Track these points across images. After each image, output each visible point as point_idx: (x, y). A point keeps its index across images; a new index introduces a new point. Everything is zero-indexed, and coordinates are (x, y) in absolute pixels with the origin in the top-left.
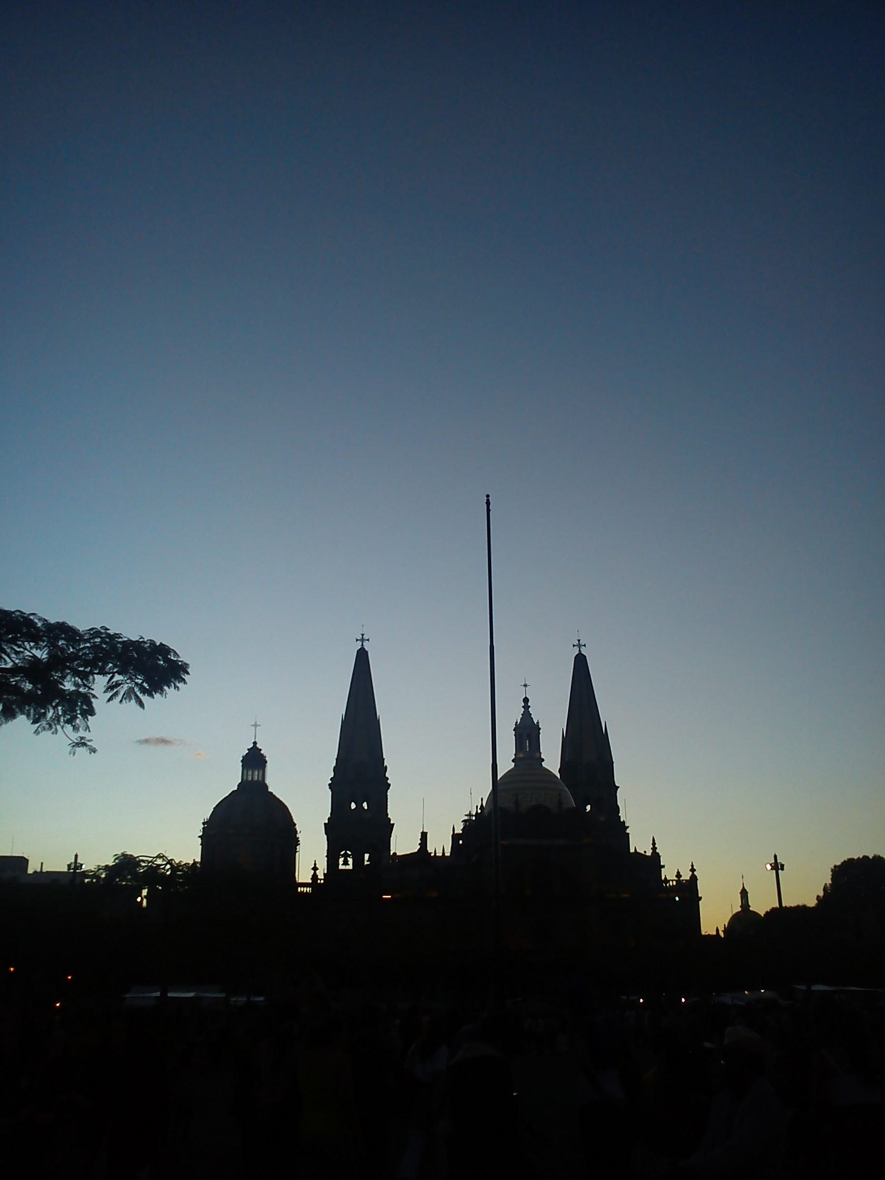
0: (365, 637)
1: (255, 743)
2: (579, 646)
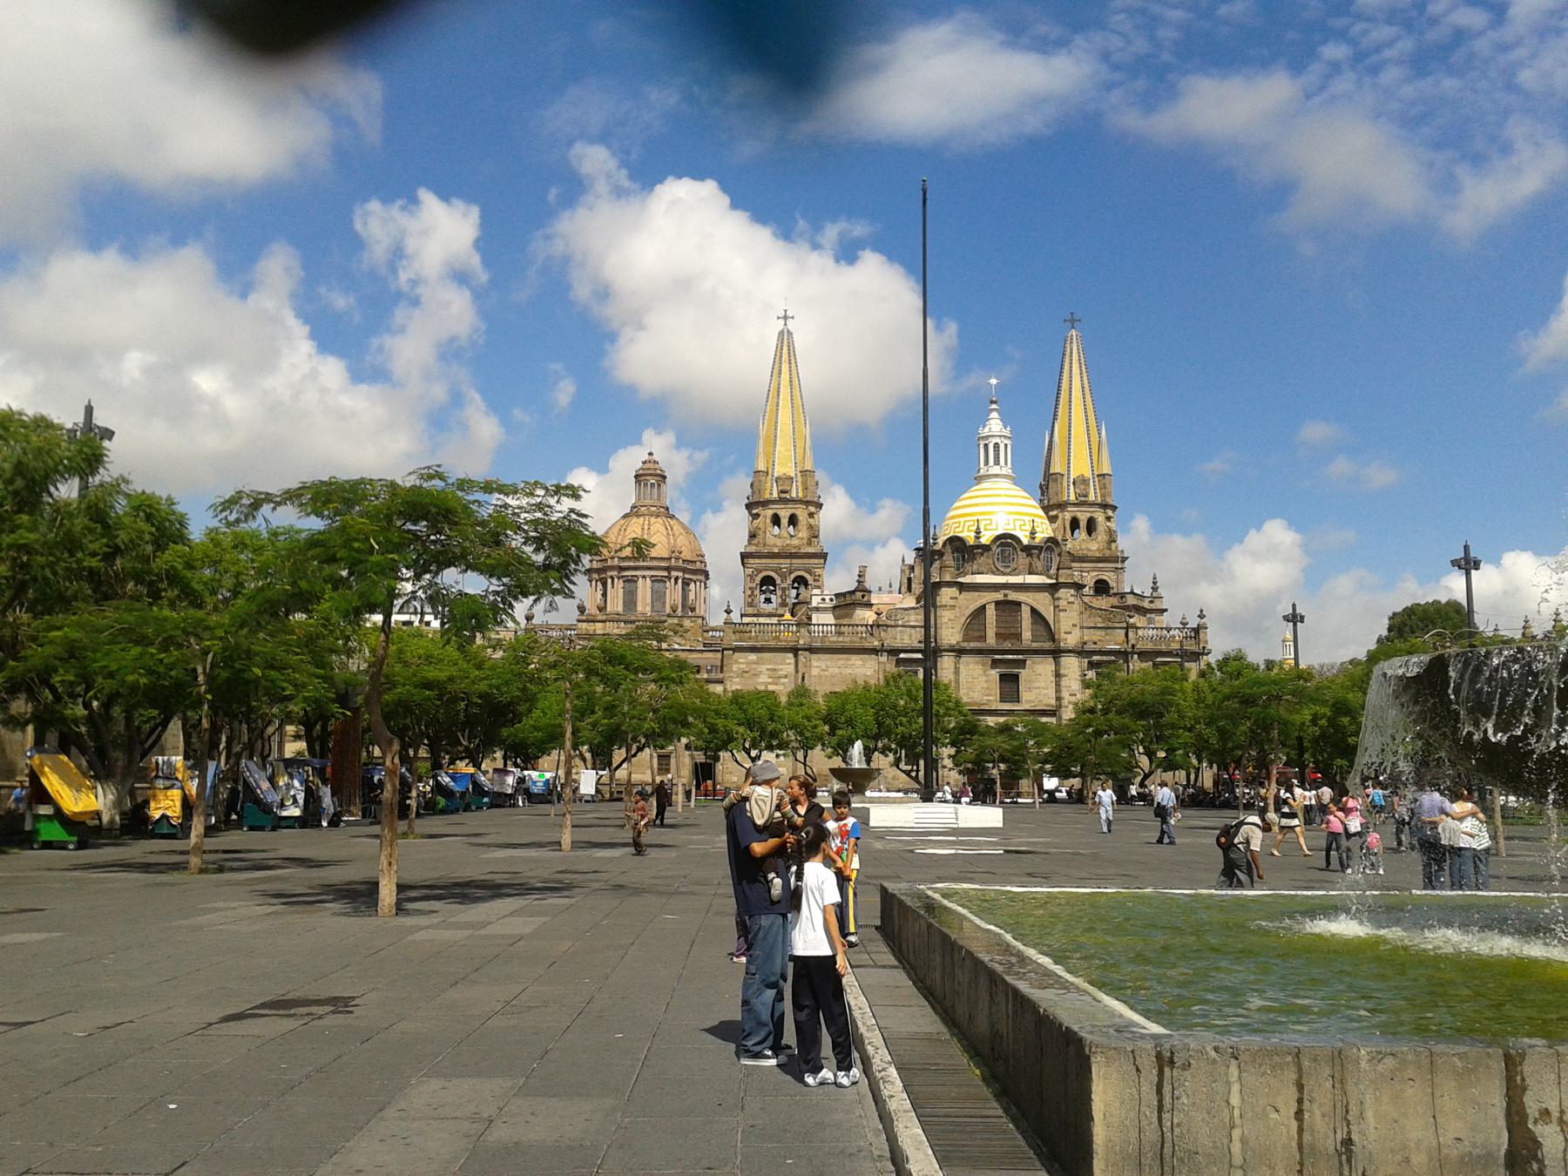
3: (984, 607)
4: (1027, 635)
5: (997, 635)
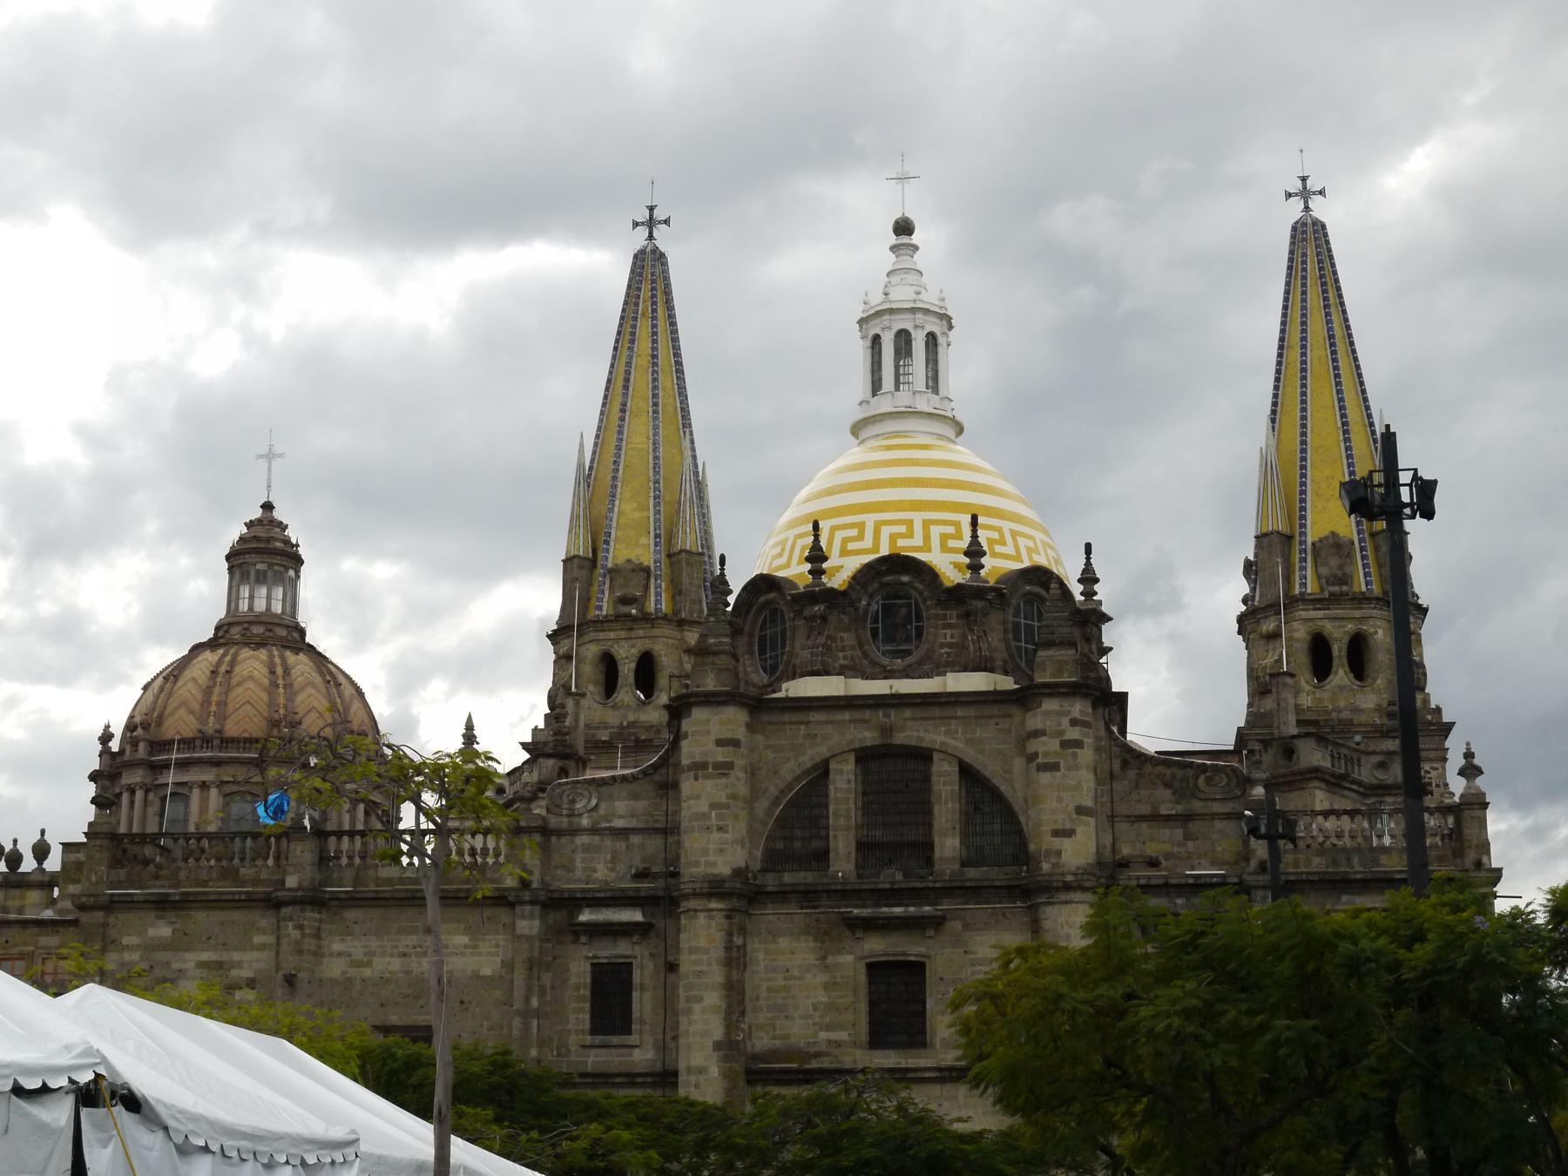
0: (659, 214)
1: (268, 507)
2: (1305, 194)
3: (822, 772)
4: (948, 845)
5: (863, 847)
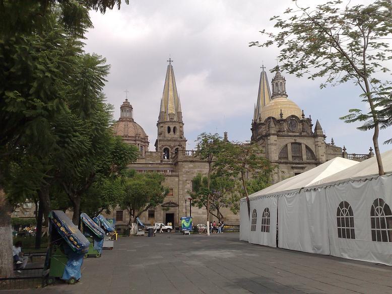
1: (127, 100)
3: (286, 145)
4: (304, 157)
